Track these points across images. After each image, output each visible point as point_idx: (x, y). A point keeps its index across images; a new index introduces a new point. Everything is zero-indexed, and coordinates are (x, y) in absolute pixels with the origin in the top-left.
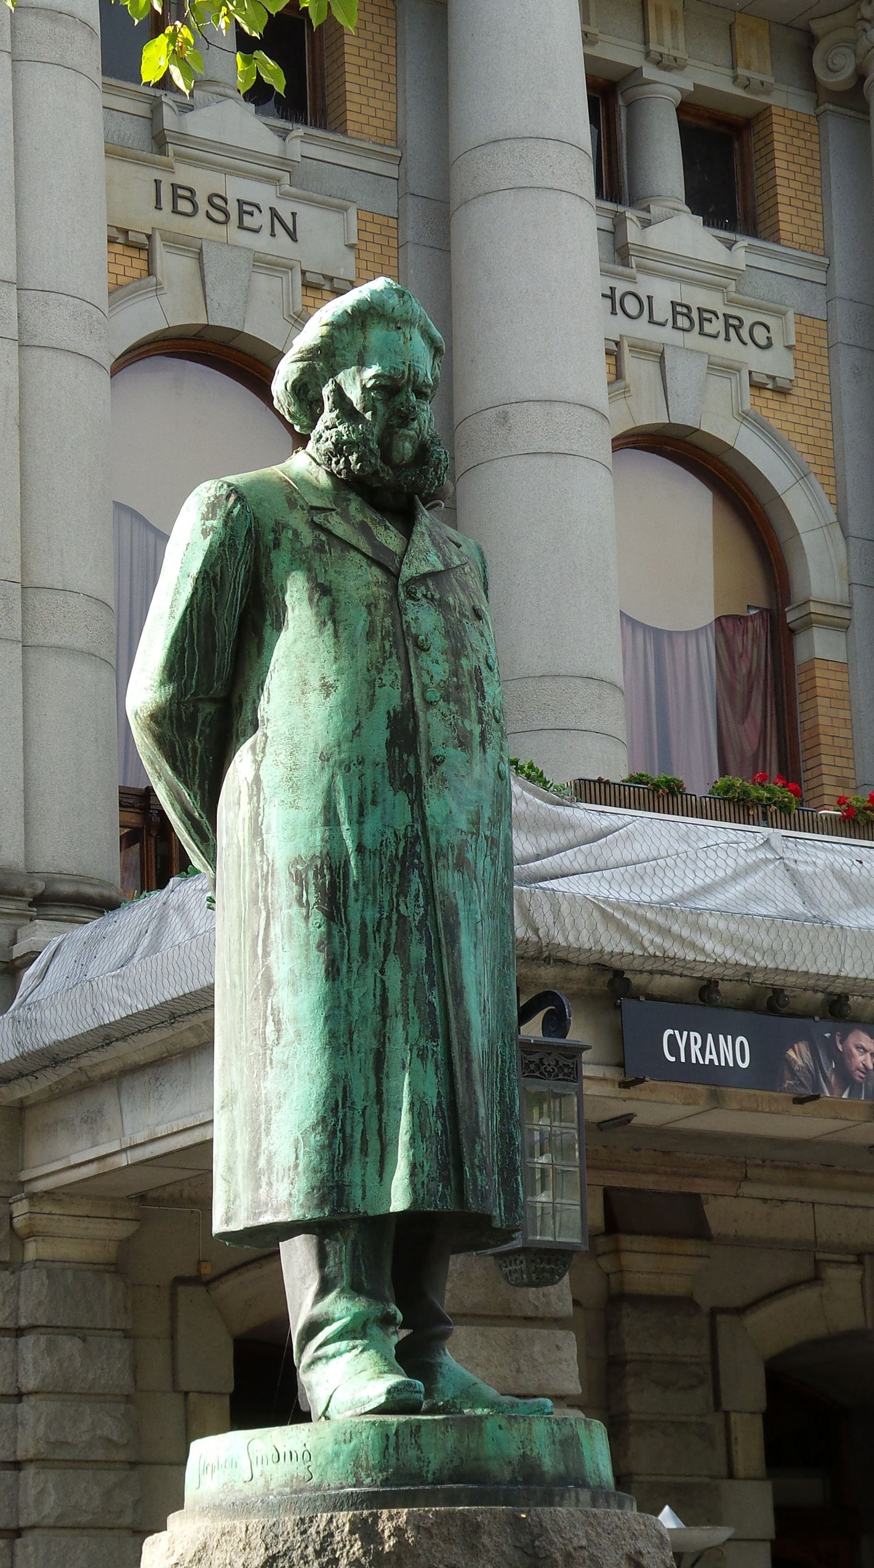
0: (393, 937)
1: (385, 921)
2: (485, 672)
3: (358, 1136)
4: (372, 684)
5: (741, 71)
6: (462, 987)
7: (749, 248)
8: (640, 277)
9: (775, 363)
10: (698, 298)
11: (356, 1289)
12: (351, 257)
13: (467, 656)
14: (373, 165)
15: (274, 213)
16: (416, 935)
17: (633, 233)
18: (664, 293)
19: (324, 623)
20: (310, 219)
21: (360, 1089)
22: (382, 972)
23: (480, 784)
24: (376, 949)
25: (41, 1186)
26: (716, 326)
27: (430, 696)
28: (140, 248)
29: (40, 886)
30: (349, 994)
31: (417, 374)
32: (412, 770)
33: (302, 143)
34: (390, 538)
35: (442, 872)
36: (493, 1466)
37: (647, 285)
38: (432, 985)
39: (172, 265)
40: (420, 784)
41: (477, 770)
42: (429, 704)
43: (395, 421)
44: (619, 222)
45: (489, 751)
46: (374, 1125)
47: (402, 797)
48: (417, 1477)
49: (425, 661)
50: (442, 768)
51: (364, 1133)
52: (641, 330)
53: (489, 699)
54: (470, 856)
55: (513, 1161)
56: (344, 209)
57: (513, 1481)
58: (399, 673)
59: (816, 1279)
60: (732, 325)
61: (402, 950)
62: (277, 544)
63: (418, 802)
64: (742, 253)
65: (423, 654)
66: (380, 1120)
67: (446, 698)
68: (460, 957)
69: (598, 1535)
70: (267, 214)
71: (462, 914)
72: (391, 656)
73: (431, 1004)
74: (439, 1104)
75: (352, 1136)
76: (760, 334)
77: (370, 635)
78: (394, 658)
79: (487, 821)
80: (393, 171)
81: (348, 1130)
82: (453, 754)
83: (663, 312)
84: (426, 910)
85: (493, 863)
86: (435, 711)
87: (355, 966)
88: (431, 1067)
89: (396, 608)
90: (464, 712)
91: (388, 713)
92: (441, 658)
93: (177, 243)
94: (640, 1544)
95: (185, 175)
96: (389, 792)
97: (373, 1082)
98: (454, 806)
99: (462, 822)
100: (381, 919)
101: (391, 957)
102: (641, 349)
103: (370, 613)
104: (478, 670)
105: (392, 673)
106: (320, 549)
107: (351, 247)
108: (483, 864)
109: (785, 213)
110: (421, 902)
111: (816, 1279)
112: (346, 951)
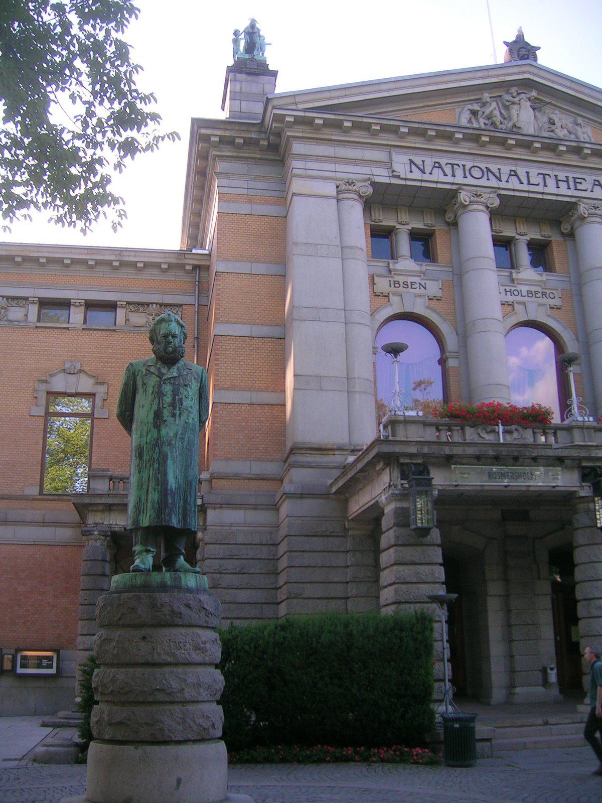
7: (546, 275)
8: (518, 286)
9: (557, 302)
10: (534, 289)
12: (440, 291)
14: (446, 269)
15: (420, 284)
17: (514, 276)
18: (524, 289)
20: (429, 284)
24: (148, 466)
25: (350, 518)
26: (540, 295)
27: (164, 406)
28: (386, 296)
29: (352, 448)
33: (427, 267)
34: (164, 371)
37: (519, 288)
39: (394, 299)
41: (177, 422)
44: (511, 273)
45: (182, 418)
49: (165, 398)
52: (519, 298)
53: (184, 405)
54: (173, 442)
60: (544, 294)
61: (153, 465)
63: (159, 431)
64: (545, 277)
70: (418, 284)
76: (552, 296)
80: (451, 270)
82: (170, 419)
83: (524, 293)
85: (182, 443)
88: (156, 492)
89: (160, 386)
90: (175, 409)
93: (395, 294)
94: (189, 602)
95: (397, 278)
98: (169, 431)
99: (171, 434)
102: (519, 303)
105: (157, 401)
106: (146, 375)
108: (178, 444)
109: (557, 265)
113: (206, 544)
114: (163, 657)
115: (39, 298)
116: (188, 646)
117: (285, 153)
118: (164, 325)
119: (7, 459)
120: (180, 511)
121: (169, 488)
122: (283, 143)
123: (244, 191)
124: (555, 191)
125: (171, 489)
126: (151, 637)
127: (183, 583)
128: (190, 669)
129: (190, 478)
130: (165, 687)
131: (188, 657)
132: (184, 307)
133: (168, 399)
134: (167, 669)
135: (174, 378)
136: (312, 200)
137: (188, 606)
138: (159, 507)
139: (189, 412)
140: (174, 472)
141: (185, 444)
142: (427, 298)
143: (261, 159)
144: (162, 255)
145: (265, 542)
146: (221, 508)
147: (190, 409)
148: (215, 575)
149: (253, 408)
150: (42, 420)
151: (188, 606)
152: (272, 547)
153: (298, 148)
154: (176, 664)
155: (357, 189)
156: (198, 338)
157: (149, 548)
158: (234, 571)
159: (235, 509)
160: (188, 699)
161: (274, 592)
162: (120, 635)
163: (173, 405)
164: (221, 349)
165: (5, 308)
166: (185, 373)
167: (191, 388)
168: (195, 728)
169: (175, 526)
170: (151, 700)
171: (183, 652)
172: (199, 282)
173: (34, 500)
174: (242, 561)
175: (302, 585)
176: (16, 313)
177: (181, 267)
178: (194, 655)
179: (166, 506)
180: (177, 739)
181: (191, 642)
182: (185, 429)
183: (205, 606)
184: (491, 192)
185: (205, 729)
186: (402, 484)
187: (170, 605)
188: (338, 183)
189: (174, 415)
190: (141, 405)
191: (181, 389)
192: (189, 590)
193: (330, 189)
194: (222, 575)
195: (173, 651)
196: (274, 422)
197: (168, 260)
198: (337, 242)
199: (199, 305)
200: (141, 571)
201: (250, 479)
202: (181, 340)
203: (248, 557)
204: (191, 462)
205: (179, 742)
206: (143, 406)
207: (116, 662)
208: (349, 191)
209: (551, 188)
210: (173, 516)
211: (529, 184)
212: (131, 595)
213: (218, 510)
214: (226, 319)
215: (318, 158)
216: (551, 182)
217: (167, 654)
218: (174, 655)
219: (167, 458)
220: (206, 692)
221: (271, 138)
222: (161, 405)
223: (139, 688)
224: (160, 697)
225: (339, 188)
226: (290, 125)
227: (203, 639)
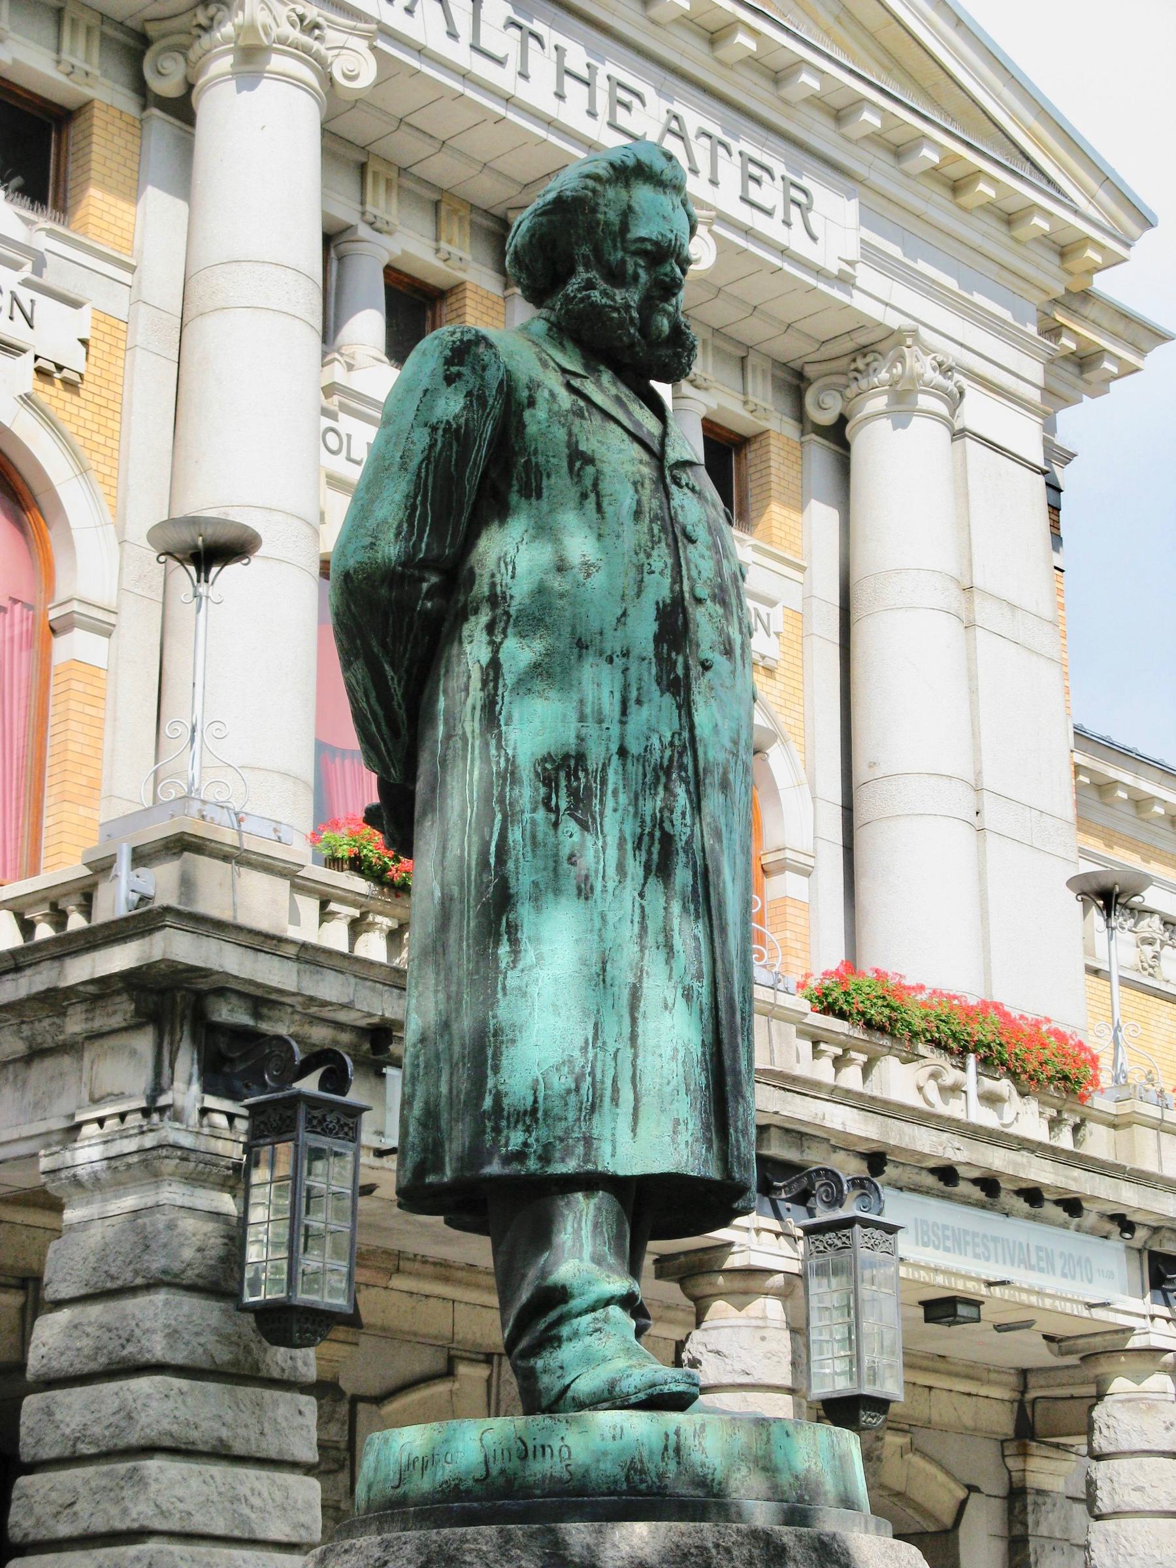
0: (655, 856)
1: (646, 839)
3: (609, 1082)
5: (443, 245)
8: (342, 416)
15: (15, 298)
16: (681, 858)
19: (584, 496)
20: (45, 307)
22: (641, 895)
30: (603, 917)
32: (680, 671)
40: (688, 689)
42: (699, 601)
43: (656, 293)
46: (627, 1073)
47: (668, 697)
51: (615, 1081)
56: (76, 304)
59: (449, 1373)
62: (532, 403)
63: (686, 708)
66: (634, 1066)
72: (659, 542)
75: (603, 1082)
77: (638, 514)
78: (663, 544)
81: (599, 1076)
84: (692, 831)
86: (703, 610)
87: (611, 885)
91: (657, 603)
92: (707, 553)
100: (642, 835)
103: (637, 491)
105: (661, 558)
107: (84, 342)
111: (449, 1373)
112: (601, 867)
118: (643, 194)
124: (548, 105)
142: (32, 365)
184: (352, 31)
186: (204, 1112)
209: (537, 92)
211: (475, 48)
216: (542, 64)
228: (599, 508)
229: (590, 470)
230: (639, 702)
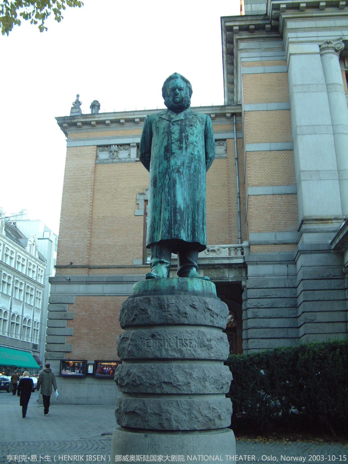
2: (189, 135)
3: (156, 227)
4: (162, 142)
6: (176, 195)
11: (156, 257)
13: (185, 133)
21: (157, 218)
22: (161, 195)
23: (184, 156)
27: (173, 141)
29: (345, 217)
31: (178, 86)
34: (173, 116)
35: (173, 174)
36: (162, 288)
38: (169, 196)
41: (184, 153)
45: (188, 150)
47: (166, 161)
48: (147, 291)
50: (175, 154)
53: (189, 140)
54: (181, 170)
55: (195, 229)
57: (166, 290)
58: (167, 139)
62: (153, 122)
65: (173, 134)
67: (177, 141)
68: (176, 189)
69: (179, 301)
71: (178, 181)
73: (168, 199)
74: (169, 218)
77: (163, 133)
79: (187, 163)
88: (167, 211)
89: (169, 127)
90: (181, 143)
92: (177, 134)
96: (164, 161)
97: (159, 217)
99: (179, 163)
101: (163, 192)
104: (188, 135)
106: (159, 121)
110: (168, 180)
113: (248, 289)
114: (171, 353)
115: (137, 143)
116: (194, 343)
117: (283, 31)
119: (121, 243)
120: (189, 227)
121: (178, 207)
122: (281, 24)
123: (258, 59)
125: (180, 208)
126: (160, 335)
127: (190, 288)
128: (195, 364)
129: (197, 200)
130: (172, 381)
131: (193, 353)
132: (227, 140)
133: (176, 136)
134: (174, 364)
135: (181, 120)
136: (303, 56)
137: (193, 307)
138: (169, 223)
139: (195, 146)
140: (183, 194)
141: (192, 172)
143: (267, 37)
144: (210, 109)
145: (288, 286)
146: (257, 264)
147: (195, 143)
148: (255, 309)
149: (274, 197)
150: (142, 218)
151: (193, 307)
152: (293, 289)
153: (290, 25)
154: (183, 360)
155: (334, 46)
156: (237, 159)
157: (162, 260)
158: (268, 306)
159: (266, 264)
160: (194, 392)
161: (295, 319)
162: (133, 334)
163: (180, 141)
164: (251, 160)
165: (117, 152)
166: (191, 117)
167: (196, 127)
168: (201, 419)
169: (185, 239)
170: (160, 392)
171: (189, 348)
172: (236, 123)
173: (139, 267)
174: (272, 299)
175: (314, 314)
176: (123, 154)
177: (224, 115)
178: (199, 350)
179: (176, 222)
180: (183, 429)
181: (197, 339)
182: (191, 160)
183: (210, 307)
185: (210, 420)
187: (176, 306)
188: (320, 43)
189: (181, 148)
190: (155, 144)
191: (187, 128)
192: (195, 293)
193: (315, 48)
194: (260, 309)
195: (179, 347)
196: (290, 205)
197: (215, 112)
198: (323, 81)
199: (237, 138)
200: (153, 278)
201: (275, 244)
202: (187, 93)
203: (277, 297)
204: (198, 186)
205: (185, 432)
206: (156, 145)
207: (130, 357)
208: (328, 48)
210: (182, 231)
212: (142, 298)
213: (255, 266)
214: (253, 141)
215: (304, 30)
217: (175, 350)
218: (181, 351)
219: (176, 183)
220: (213, 386)
221: (273, 22)
222: (170, 141)
223: (149, 381)
224: (167, 389)
225: (321, 47)
226: (284, 10)
227: (209, 337)
228: (158, 135)
229: (158, 129)
230: (161, 164)
